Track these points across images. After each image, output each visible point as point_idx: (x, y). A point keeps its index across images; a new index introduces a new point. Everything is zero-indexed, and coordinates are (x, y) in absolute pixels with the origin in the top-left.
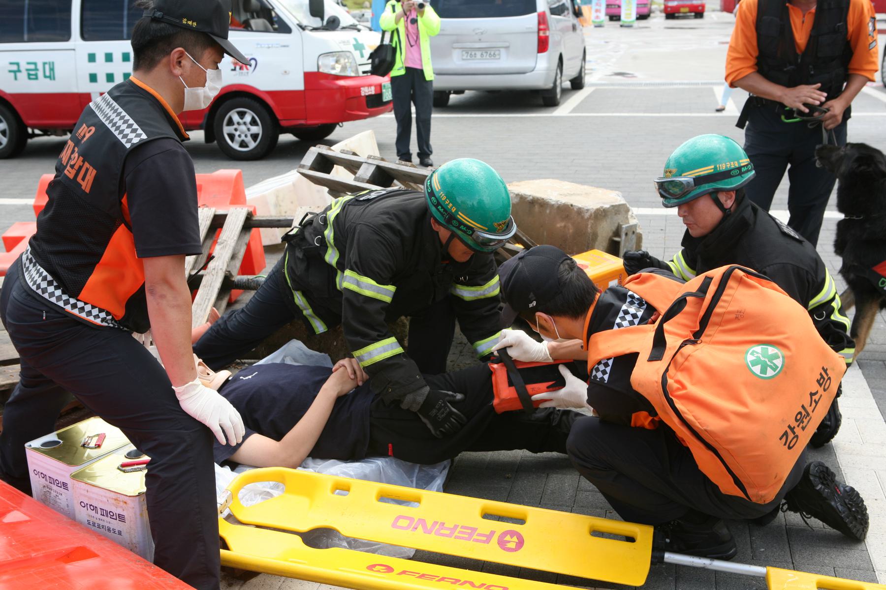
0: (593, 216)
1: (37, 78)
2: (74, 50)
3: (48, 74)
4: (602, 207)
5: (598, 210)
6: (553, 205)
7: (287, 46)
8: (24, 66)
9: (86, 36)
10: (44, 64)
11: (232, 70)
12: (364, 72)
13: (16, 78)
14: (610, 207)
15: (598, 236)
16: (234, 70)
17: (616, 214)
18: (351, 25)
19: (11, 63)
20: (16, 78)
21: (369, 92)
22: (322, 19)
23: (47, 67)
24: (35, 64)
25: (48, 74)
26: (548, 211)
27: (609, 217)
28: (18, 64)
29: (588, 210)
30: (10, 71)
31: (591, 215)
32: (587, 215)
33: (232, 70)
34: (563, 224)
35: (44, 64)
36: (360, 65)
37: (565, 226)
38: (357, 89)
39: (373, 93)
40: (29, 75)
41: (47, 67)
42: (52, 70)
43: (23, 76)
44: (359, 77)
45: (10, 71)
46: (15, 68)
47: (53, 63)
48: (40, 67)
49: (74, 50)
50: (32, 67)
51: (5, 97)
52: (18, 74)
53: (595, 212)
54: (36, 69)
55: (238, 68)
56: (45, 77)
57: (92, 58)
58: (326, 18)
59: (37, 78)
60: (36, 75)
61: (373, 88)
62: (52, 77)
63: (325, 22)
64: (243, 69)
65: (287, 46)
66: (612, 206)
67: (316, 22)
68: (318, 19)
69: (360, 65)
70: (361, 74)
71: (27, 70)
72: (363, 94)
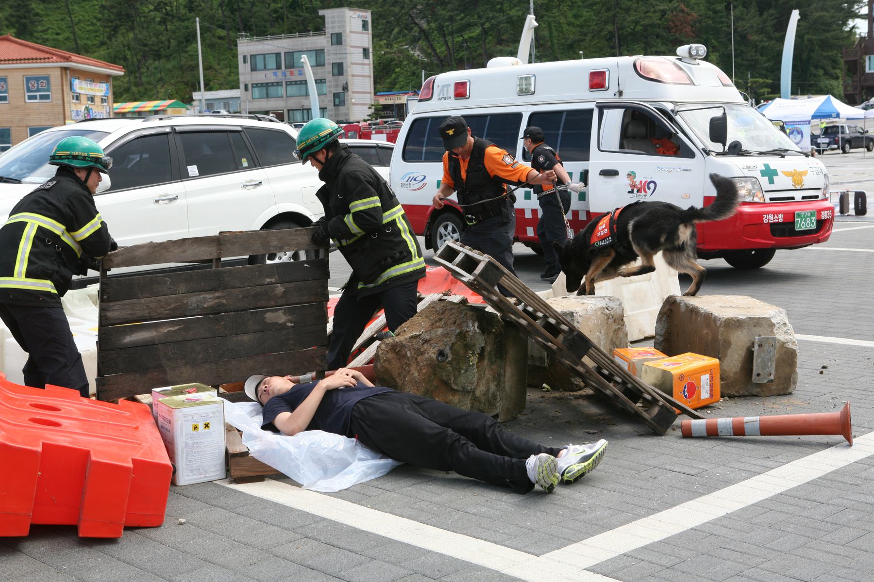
0: (723, 324)
4: (736, 318)
5: (729, 319)
6: (702, 313)
7: (690, 170)
9: (407, 157)
11: (629, 192)
12: (771, 199)
14: (747, 318)
15: (731, 344)
16: (632, 192)
17: (755, 326)
18: (774, 151)
21: (774, 220)
22: (724, 145)
26: (699, 319)
27: (746, 328)
29: (720, 319)
31: (721, 323)
32: (718, 323)
33: (629, 192)
34: (706, 331)
36: (766, 191)
37: (707, 333)
38: (760, 215)
39: (781, 220)
44: (765, 203)
53: (725, 321)
55: (635, 190)
58: (728, 143)
61: (781, 216)
63: (727, 148)
64: (641, 192)
65: (690, 170)
66: (750, 318)
67: (718, 147)
68: (720, 145)
69: (766, 191)
70: (768, 201)
72: (766, 221)
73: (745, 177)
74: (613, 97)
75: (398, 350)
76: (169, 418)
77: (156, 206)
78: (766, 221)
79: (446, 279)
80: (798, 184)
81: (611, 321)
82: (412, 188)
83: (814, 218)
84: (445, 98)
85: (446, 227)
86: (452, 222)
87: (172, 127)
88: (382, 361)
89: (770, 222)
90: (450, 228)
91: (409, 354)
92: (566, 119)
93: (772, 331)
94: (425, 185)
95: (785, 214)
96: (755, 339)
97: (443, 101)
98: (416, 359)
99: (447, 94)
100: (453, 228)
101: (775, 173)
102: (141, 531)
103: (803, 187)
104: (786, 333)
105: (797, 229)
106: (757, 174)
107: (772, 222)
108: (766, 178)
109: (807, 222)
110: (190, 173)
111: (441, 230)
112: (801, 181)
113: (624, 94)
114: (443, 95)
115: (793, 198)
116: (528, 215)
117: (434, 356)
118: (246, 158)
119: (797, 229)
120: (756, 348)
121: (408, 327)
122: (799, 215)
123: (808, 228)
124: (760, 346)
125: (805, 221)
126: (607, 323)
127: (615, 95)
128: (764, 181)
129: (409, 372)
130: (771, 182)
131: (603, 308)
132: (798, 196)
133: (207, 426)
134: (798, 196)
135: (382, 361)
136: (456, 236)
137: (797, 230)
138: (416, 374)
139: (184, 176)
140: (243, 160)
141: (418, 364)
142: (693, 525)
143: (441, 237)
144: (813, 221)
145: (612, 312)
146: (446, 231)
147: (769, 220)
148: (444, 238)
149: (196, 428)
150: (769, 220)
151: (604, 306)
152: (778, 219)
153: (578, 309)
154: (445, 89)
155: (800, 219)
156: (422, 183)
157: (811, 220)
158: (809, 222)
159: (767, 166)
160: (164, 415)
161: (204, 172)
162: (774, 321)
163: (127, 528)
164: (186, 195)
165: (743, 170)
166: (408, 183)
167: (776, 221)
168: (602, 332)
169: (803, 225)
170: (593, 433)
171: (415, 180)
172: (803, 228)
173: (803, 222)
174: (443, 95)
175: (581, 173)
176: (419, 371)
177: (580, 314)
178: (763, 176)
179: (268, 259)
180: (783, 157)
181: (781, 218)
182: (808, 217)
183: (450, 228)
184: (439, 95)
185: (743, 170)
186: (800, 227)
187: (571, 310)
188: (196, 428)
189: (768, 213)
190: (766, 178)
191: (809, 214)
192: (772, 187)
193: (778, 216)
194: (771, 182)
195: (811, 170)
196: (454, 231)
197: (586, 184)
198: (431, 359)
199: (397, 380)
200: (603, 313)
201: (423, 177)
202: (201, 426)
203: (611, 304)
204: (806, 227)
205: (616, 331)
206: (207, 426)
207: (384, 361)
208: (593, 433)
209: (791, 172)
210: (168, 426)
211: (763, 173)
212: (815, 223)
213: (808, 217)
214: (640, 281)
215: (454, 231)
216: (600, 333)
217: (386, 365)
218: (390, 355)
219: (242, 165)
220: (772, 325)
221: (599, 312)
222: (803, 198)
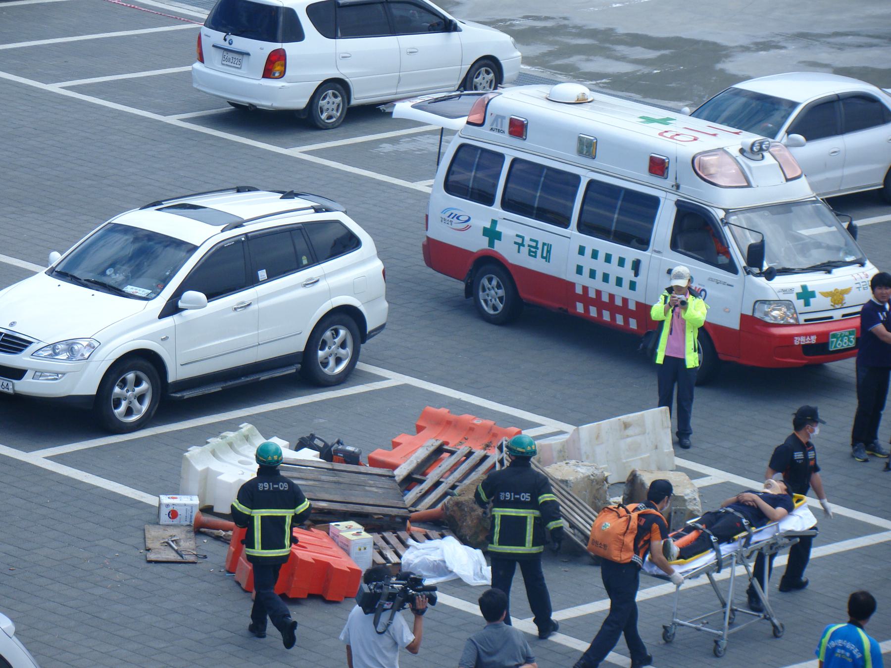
1: (535, 257)
2: (570, 238)
3: (545, 255)
8: (527, 242)
10: (544, 244)
12: (806, 321)
13: (519, 252)
17: (674, 500)
19: (517, 236)
20: (519, 252)
21: (806, 341)
23: (546, 247)
24: (537, 242)
25: (545, 255)
28: (523, 238)
30: (516, 243)
35: (544, 244)
36: (800, 314)
38: (791, 337)
40: (530, 251)
41: (546, 247)
42: (549, 252)
43: (525, 250)
45: (516, 243)
46: (519, 240)
47: (551, 245)
48: (540, 246)
49: (570, 238)
50: (534, 244)
51: (508, 266)
52: (521, 247)
54: (536, 247)
56: (542, 257)
57: (582, 251)
59: (535, 257)
60: (535, 252)
62: (547, 258)
69: (800, 314)
71: (529, 246)
72: (796, 343)
73: (780, 300)
74: (671, 188)
75: (460, 505)
76: (347, 544)
77: (235, 313)
78: (796, 343)
79: (489, 433)
80: (838, 304)
81: (594, 483)
82: (454, 226)
83: (853, 336)
84: (499, 131)
85: (490, 280)
86: (498, 277)
87: (246, 234)
88: (450, 511)
89: (802, 343)
90: (494, 283)
91: (466, 509)
92: (621, 206)
93: (685, 504)
94: (469, 227)
95: (819, 335)
96: (671, 509)
97: (495, 134)
98: (470, 513)
99: (501, 128)
100: (498, 283)
101: (812, 294)
102: (348, 599)
103: (845, 306)
104: (695, 504)
105: (832, 348)
106: (793, 297)
107: (804, 343)
108: (802, 301)
109: (845, 341)
110: (260, 278)
111: (485, 281)
112: (842, 299)
113: (681, 188)
114: (497, 126)
115: (831, 318)
116: (579, 291)
117: (481, 514)
118: (306, 256)
119: (832, 348)
120: (673, 514)
121: (466, 491)
122: (834, 336)
123: (845, 346)
124: (675, 513)
125: (842, 341)
126: (592, 485)
127: (673, 186)
128: (799, 304)
129: (466, 520)
130: (807, 304)
131: (589, 476)
132: (837, 314)
133: (365, 549)
134: (837, 314)
135: (450, 511)
136: (501, 292)
137: (831, 350)
138: (470, 523)
139: (253, 281)
140: (303, 258)
141: (471, 516)
142: (591, 612)
143: (484, 290)
144: (852, 339)
145: (596, 478)
146: (490, 284)
147: (800, 342)
148: (488, 291)
149: (360, 550)
150: (800, 342)
151: (590, 474)
152: (810, 341)
153: (571, 478)
154: (500, 120)
155: (835, 339)
156: (465, 225)
157: (849, 339)
158: (846, 341)
159: (804, 288)
160: (344, 542)
161: (272, 276)
162: (686, 498)
163: (345, 598)
164: (259, 299)
165: (778, 294)
166: (450, 219)
167: (808, 342)
168: (588, 491)
169: (839, 344)
170: (566, 562)
171: (458, 218)
172: (839, 347)
173: (839, 342)
174: (497, 126)
175: (633, 261)
176: (472, 521)
177: (573, 481)
178: (798, 298)
179: (320, 350)
180: (829, 272)
181: (813, 340)
182: (845, 336)
183: (494, 283)
184: (492, 124)
185: (778, 294)
186: (835, 347)
187: (567, 479)
188: (360, 550)
189: (799, 335)
190: (802, 301)
191: (847, 334)
192: (808, 309)
193: (810, 338)
194: (807, 304)
195: (858, 286)
196: (499, 287)
197: (636, 275)
198: (478, 515)
199: (458, 522)
200: (589, 479)
201: (467, 218)
202: (362, 549)
203: (596, 472)
204: (842, 346)
205: (598, 490)
206: (365, 549)
207: (451, 511)
208: (566, 562)
209: (831, 292)
210: (345, 547)
211: (799, 296)
212: (854, 342)
213: (845, 336)
214: (635, 436)
215: (499, 287)
216: (586, 492)
217: (452, 513)
218: (455, 508)
219: (303, 263)
220: (685, 501)
221: (586, 479)
222: (844, 316)
